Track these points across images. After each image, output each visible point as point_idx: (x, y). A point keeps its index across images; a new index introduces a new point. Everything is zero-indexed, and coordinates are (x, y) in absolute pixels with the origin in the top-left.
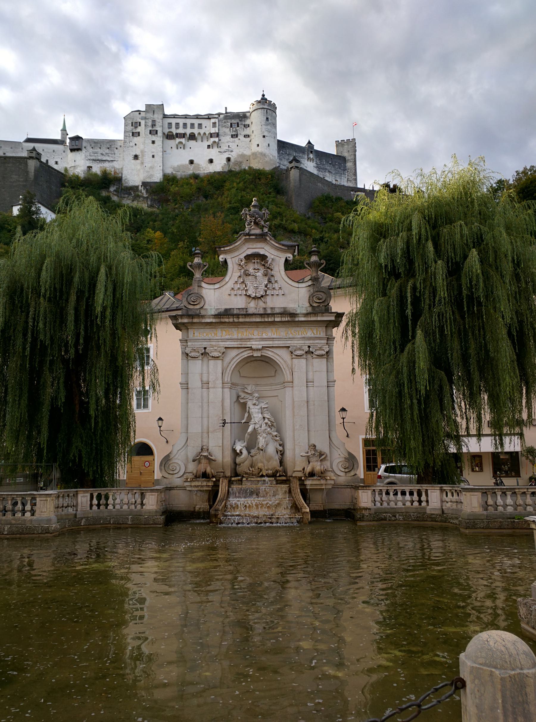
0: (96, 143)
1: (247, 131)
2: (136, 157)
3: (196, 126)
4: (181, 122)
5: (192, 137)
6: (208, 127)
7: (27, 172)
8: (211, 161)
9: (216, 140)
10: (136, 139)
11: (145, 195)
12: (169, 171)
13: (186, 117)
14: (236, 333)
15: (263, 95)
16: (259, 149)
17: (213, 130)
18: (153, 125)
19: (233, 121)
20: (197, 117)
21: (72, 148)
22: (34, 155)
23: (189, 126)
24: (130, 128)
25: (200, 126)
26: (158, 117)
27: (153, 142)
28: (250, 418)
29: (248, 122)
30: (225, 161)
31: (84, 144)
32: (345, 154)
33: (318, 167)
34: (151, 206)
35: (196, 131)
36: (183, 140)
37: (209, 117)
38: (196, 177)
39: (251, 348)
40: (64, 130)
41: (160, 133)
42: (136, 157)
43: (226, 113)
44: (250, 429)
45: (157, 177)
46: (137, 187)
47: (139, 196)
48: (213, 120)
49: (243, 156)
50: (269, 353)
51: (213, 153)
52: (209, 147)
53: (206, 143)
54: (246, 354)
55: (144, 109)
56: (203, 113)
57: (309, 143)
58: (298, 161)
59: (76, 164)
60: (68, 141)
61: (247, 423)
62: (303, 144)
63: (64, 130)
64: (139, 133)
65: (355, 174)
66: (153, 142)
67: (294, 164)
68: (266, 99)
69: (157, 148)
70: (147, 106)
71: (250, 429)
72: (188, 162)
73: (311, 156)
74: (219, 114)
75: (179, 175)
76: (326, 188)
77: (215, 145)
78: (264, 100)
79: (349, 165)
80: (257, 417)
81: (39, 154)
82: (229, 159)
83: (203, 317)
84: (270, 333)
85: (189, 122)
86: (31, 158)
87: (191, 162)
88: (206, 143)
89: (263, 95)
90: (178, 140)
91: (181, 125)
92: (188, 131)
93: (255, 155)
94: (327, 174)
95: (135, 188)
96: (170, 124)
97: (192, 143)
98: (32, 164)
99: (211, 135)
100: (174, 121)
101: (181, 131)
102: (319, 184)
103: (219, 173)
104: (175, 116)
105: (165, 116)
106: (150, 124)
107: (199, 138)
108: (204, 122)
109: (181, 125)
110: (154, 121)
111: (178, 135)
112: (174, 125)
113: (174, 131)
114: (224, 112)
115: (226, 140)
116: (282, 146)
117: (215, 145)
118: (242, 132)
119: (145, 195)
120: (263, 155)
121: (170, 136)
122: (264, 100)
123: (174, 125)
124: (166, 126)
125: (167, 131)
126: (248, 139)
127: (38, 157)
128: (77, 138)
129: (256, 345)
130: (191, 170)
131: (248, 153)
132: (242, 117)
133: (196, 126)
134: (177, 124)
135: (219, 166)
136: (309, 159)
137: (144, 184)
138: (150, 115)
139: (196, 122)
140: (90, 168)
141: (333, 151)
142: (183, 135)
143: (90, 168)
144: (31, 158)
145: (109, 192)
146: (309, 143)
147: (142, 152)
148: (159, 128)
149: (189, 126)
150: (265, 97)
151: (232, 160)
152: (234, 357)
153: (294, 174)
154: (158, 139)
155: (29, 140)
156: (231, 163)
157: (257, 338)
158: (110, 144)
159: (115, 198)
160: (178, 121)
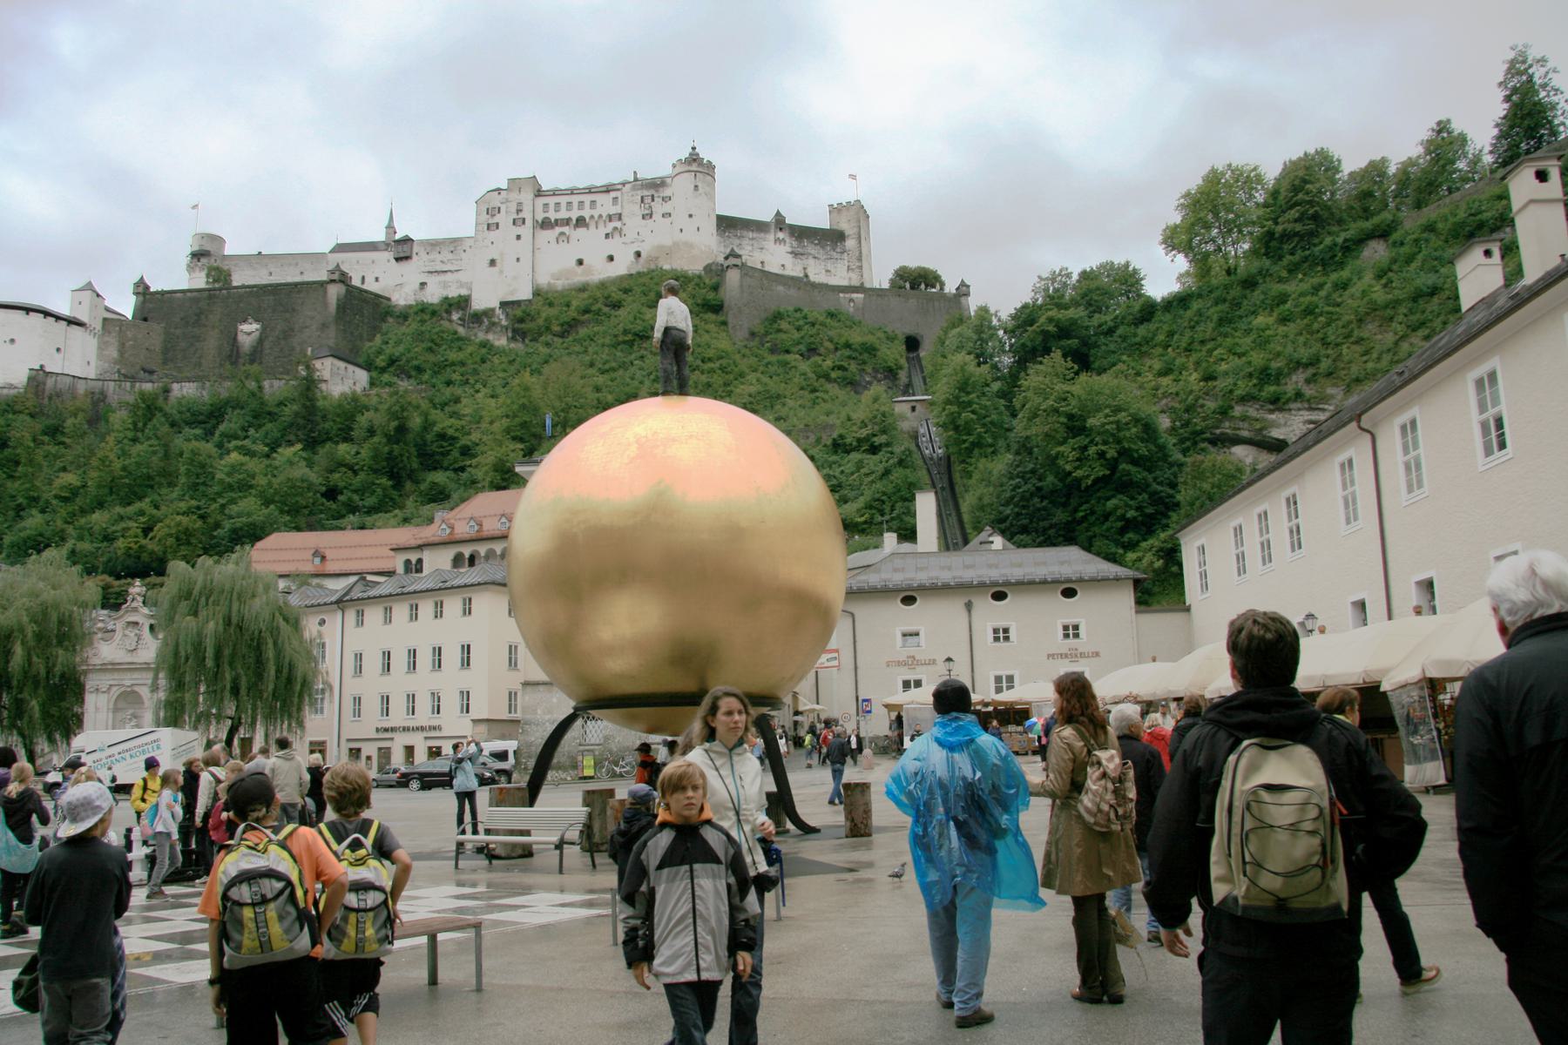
0: (434, 245)
1: (667, 208)
2: (493, 263)
3: (587, 204)
4: (563, 200)
5: (581, 222)
6: (605, 205)
7: (325, 304)
8: (611, 258)
9: (618, 224)
10: (493, 235)
11: (504, 323)
12: (544, 280)
13: (572, 192)
14: (116, 676)
16: (683, 237)
17: (614, 210)
18: (519, 211)
19: (646, 193)
20: (590, 191)
22: (336, 277)
23: (575, 205)
24: (484, 217)
25: (593, 202)
26: (527, 197)
27: (519, 237)
29: (667, 192)
30: (632, 257)
31: (415, 249)
32: (845, 226)
33: (795, 254)
34: (513, 339)
35: (586, 213)
36: (566, 229)
37: (607, 189)
38: (583, 288)
40: (390, 228)
41: (529, 222)
42: (493, 263)
43: (636, 180)
45: (525, 294)
46: (493, 310)
47: (494, 324)
48: (613, 194)
49: (660, 248)
51: (613, 246)
52: (607, 236)
53: (603, 230)
56: (600, 182)
57: (778, 213)
58: (739, 256)
59: (399, 285)
62: (767, 216)
63: (390, 228)
64: (497, 225)
65: (860, 259)
66: (519, 237)
67: (732, 261)
69: (525, 245)
70: (511, 181)
72: (574, 263)
73: (781, 235)
74: (624, 184)
75: (560, 284)
76: (793, 292)
77: (617, 235)
78: (694, 158)
79: (850, 243)
81: (343, 274)
82: (638, 254)
84: (136, 675)
85: (575, 199)
86: (333, 281)
87: (580, 262)
88: (603, 230)
90: (558, 230)
91: (563, 206)
92: (574, 215)
93: (676, 244)
94: (811, 261)
95: (488, 313)
96: (546, 205)
97: (581, 231)
98: (334, 292)
99: (610, 218)
100: (552, 201)
101: (563, 214)
102: (781, 288)
103: (622, 278)
104: (555, 193)
105: (539, 193)
106: (513, 208)
107: (592, 226)
108: (599, 198)
109: (563, 206)
110: (520, 204)
111: (557, 223)
112: (552, 207)
113: (553, 216)
115: (633, 222)
116: (727, 224)
117: (617, 235)
118: (659, 208)
119: (504, 323)
120: (690, 246)
121: (546, 224)
122: (694, 158)
123: (552, 207)
124: (539, 208)
125: (540, 217)
126: (668, 220)
127: (344, 279)
128: (407, 240)
129: (128, 683)
130: (579, 277)
131: (668, 242)
132: (657, 185)
133: (587, 204)
134: (558, 204)
135: (621, 268)
136: (777, 240)
137: (504, 305)
138: (514, 196)
139: (587, 199)
140: (423, 284)
141: (824, 223)
142: (567, 222)
143: (423, 284)
144: (333, 281)
145: (451, 321)
146: (778, 213)
147: (502, 254)
148: (527, 214)
149: (575, 205)
151: (643, 254)
152: (115, 692)
153: (733, 277)
154: (525, 232)
155: (340, 248)
156: (642, 260)
157: (128, 680)
158: (454, 243)
159: (461, 331)
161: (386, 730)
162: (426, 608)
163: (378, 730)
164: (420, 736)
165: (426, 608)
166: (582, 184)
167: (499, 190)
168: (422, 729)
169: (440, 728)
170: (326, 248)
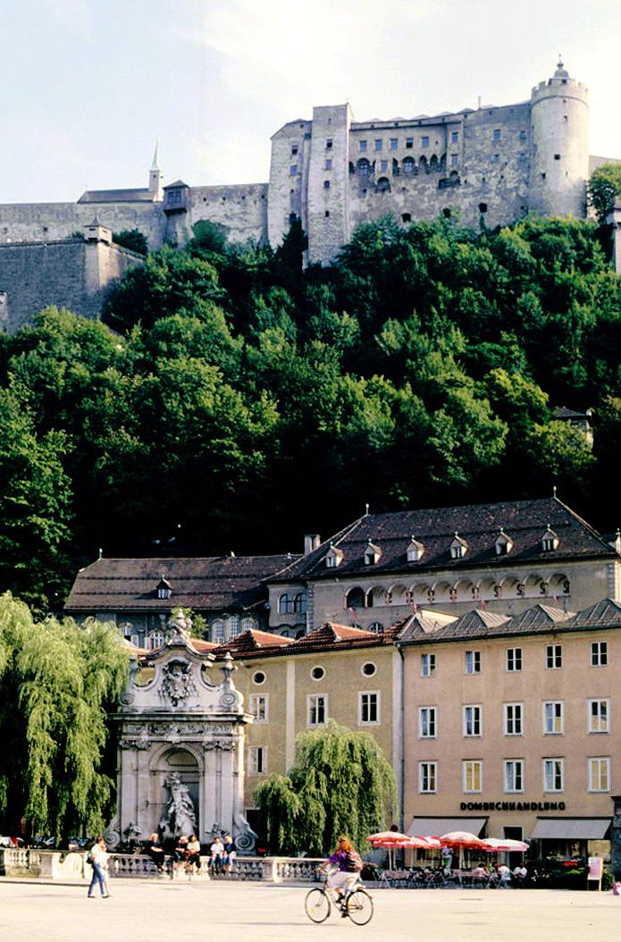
4: (386, 136)
13: (397, 126)
15: (560, 65)
21: (168, 207)
28: (173, 800)
39: (171, 742)
44: (171, 810)
50: (188, 748)
54: (169, 746)
55: (309, 117)
60: (161, 193)
61: (170, 805)
68: (566, 74)
71: (171, 810)
80: (178, 798)
83: (134, 716)
89: (560, 65)
104: (372, 127)
114: (476, 109)
150: (564, 68)
160: (378, 135)
161: (477, 807)
162: (535, 655)
163: (463, 806)
164: (531, 816)
165: (535, 655)
166: (409, 115)
167: (301, 123)
168: (535, 807)
169: (562, 806)
170: (69, 193)
